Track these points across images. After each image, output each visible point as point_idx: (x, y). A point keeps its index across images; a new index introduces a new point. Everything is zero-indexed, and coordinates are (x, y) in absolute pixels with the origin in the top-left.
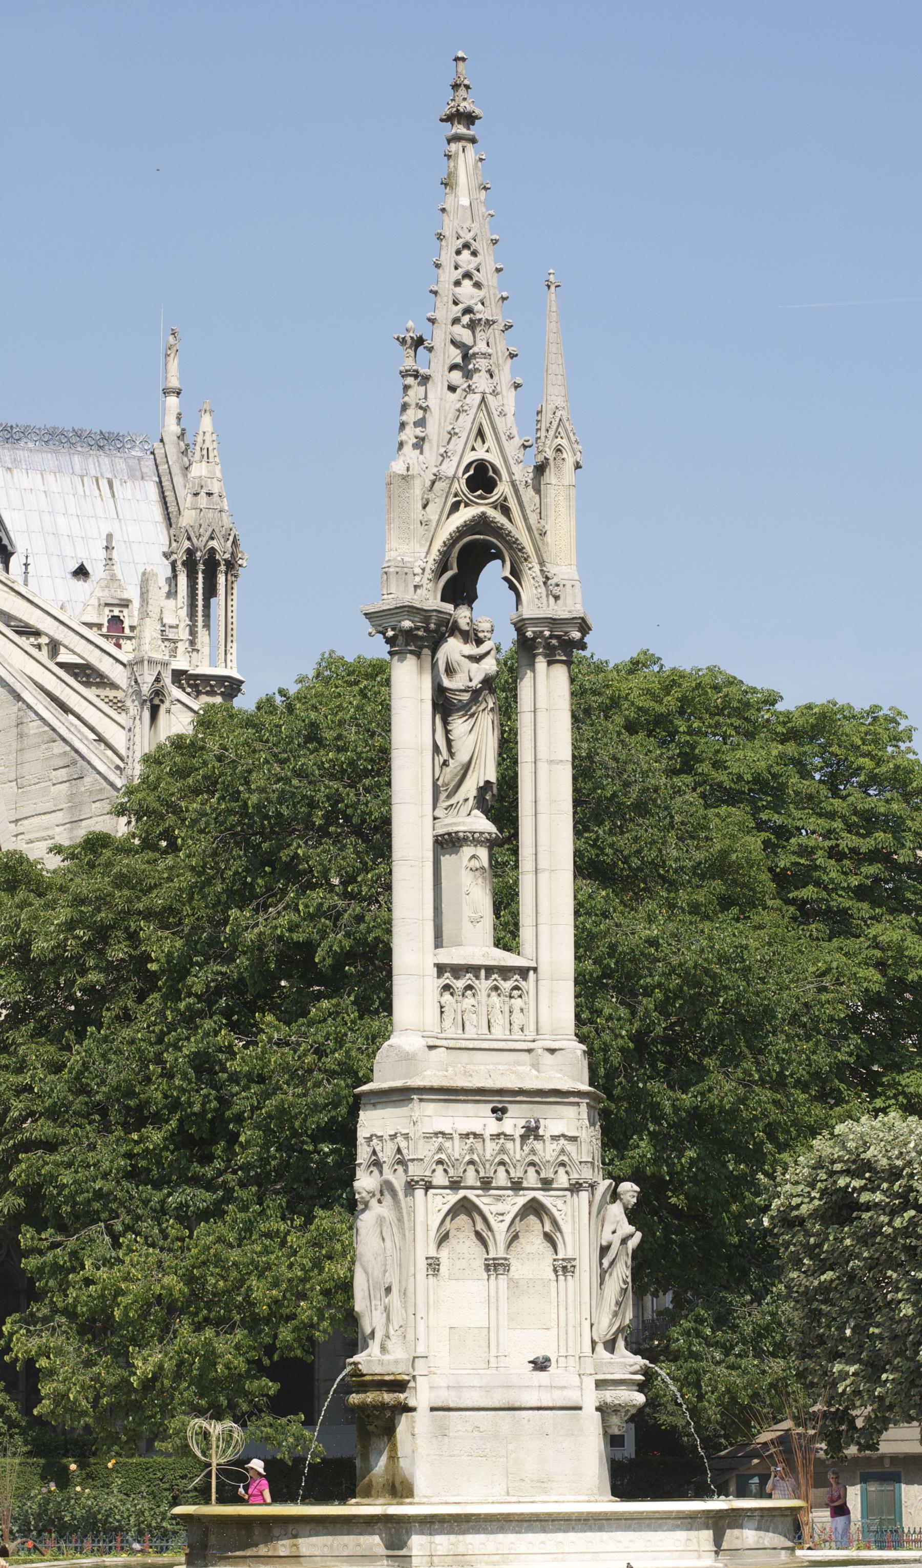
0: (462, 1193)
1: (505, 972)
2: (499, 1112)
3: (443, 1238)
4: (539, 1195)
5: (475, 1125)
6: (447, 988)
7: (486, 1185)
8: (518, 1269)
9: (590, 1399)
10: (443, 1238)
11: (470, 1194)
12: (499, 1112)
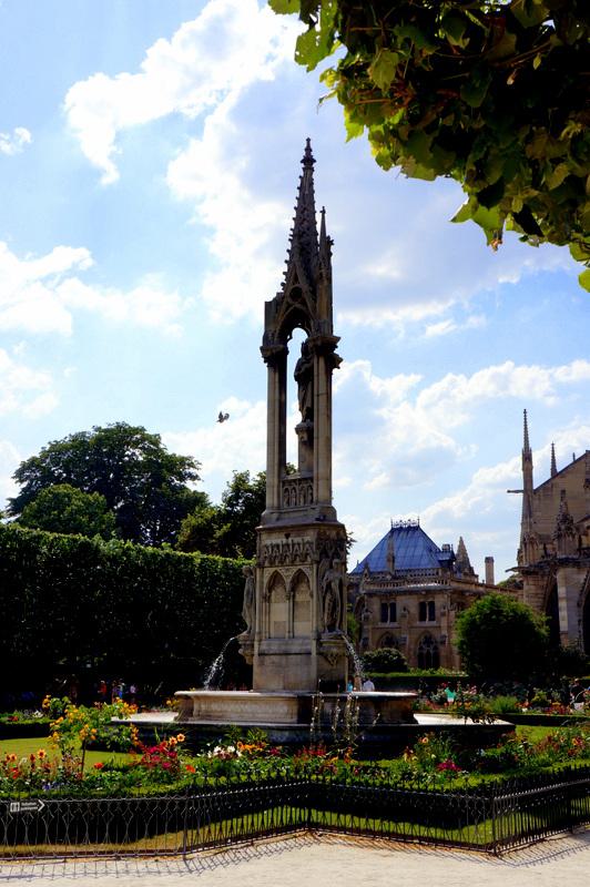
0: (274, 569)
1: (305, 479)
2: (287, 536)
3: (270, 589)
4: (301, 567)
5: (279, 541)
6: (287, 490)
7: (282, 562)
8: (299, 598)
9: (313, 647)
10: (270, 589)
11: (278, 569)
12: (287, 536)
